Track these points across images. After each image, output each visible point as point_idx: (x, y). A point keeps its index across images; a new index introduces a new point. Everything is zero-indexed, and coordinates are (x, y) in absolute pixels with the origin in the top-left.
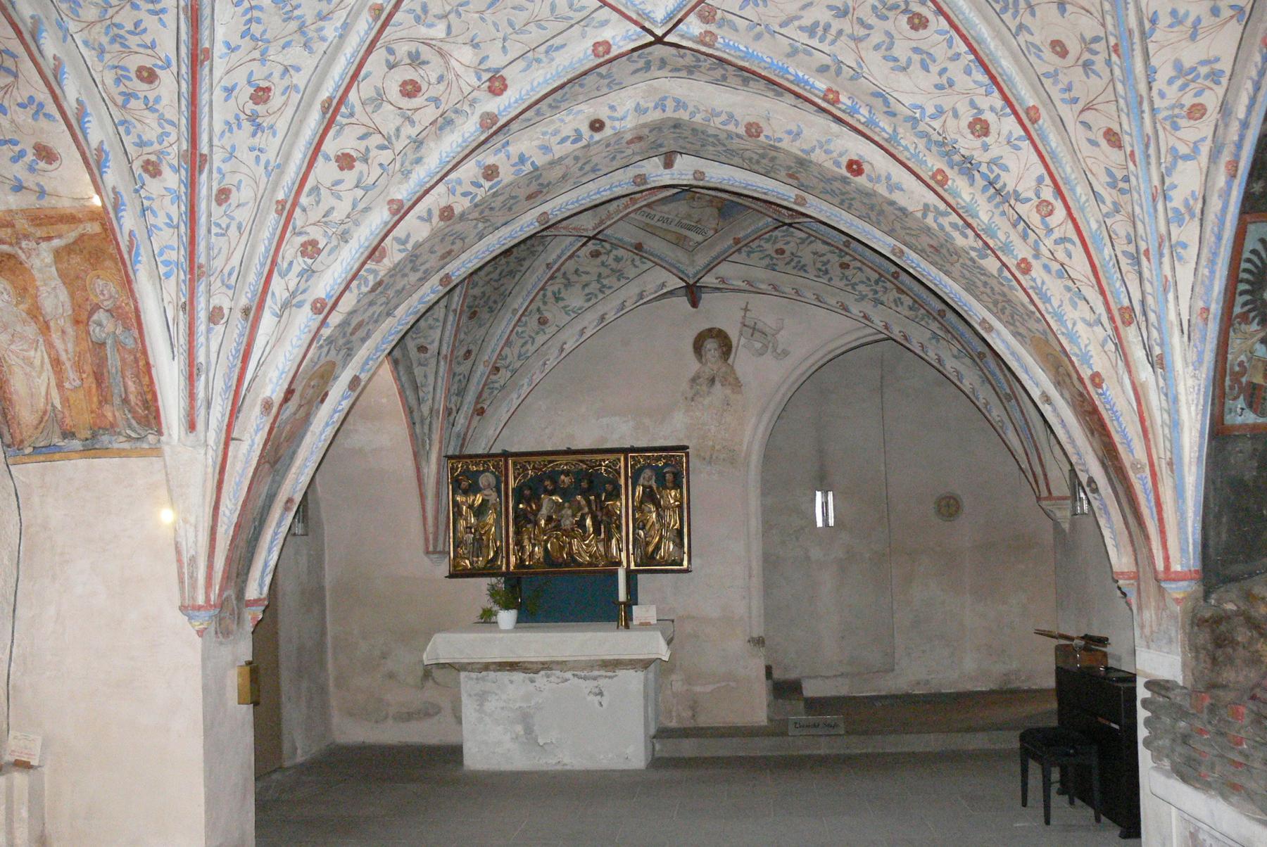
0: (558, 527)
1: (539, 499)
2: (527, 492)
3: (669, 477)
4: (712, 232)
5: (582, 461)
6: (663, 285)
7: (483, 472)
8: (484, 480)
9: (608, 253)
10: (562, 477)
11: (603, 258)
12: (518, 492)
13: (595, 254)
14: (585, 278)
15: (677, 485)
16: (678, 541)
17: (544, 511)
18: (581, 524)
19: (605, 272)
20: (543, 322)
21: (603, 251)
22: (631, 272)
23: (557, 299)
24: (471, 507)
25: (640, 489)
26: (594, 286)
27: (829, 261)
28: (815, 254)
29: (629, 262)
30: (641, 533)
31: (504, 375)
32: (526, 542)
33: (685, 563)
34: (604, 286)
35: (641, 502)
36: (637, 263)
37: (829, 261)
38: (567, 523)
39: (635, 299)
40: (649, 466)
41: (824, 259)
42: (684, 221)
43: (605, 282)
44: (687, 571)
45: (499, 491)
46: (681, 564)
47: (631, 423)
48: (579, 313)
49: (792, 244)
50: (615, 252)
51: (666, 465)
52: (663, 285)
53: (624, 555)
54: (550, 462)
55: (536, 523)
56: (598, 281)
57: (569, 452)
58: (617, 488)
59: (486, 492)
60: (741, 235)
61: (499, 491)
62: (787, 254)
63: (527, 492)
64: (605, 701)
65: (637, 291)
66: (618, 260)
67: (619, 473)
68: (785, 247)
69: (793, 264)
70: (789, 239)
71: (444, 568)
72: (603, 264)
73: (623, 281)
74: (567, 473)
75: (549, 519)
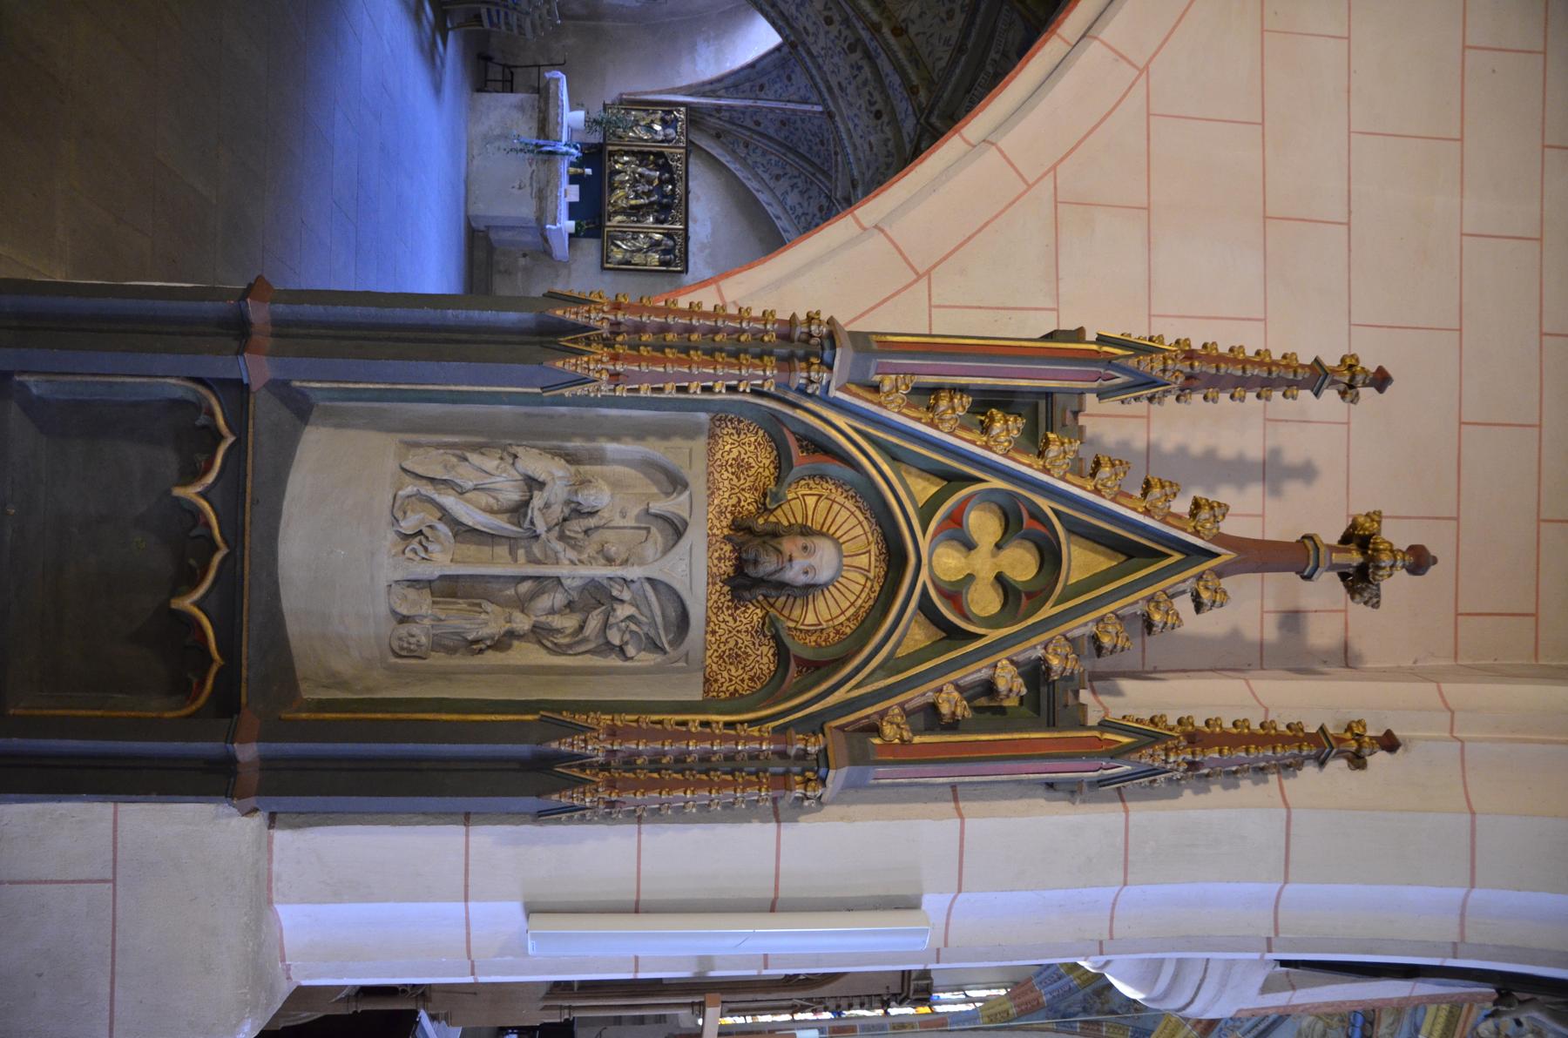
0: (636, 181)
8: (670, 131)
20: (778, 177)
23: (792, 187)
25: (657, 237)
26: (799, 211)
31: (742, 152)
38: (640, 188)
44: (603, 268)
48: (782, 203)
57: (687, 192)
64: (515, 191)
71: (608, 102)
74: (673, 190)
75: (641, 175)
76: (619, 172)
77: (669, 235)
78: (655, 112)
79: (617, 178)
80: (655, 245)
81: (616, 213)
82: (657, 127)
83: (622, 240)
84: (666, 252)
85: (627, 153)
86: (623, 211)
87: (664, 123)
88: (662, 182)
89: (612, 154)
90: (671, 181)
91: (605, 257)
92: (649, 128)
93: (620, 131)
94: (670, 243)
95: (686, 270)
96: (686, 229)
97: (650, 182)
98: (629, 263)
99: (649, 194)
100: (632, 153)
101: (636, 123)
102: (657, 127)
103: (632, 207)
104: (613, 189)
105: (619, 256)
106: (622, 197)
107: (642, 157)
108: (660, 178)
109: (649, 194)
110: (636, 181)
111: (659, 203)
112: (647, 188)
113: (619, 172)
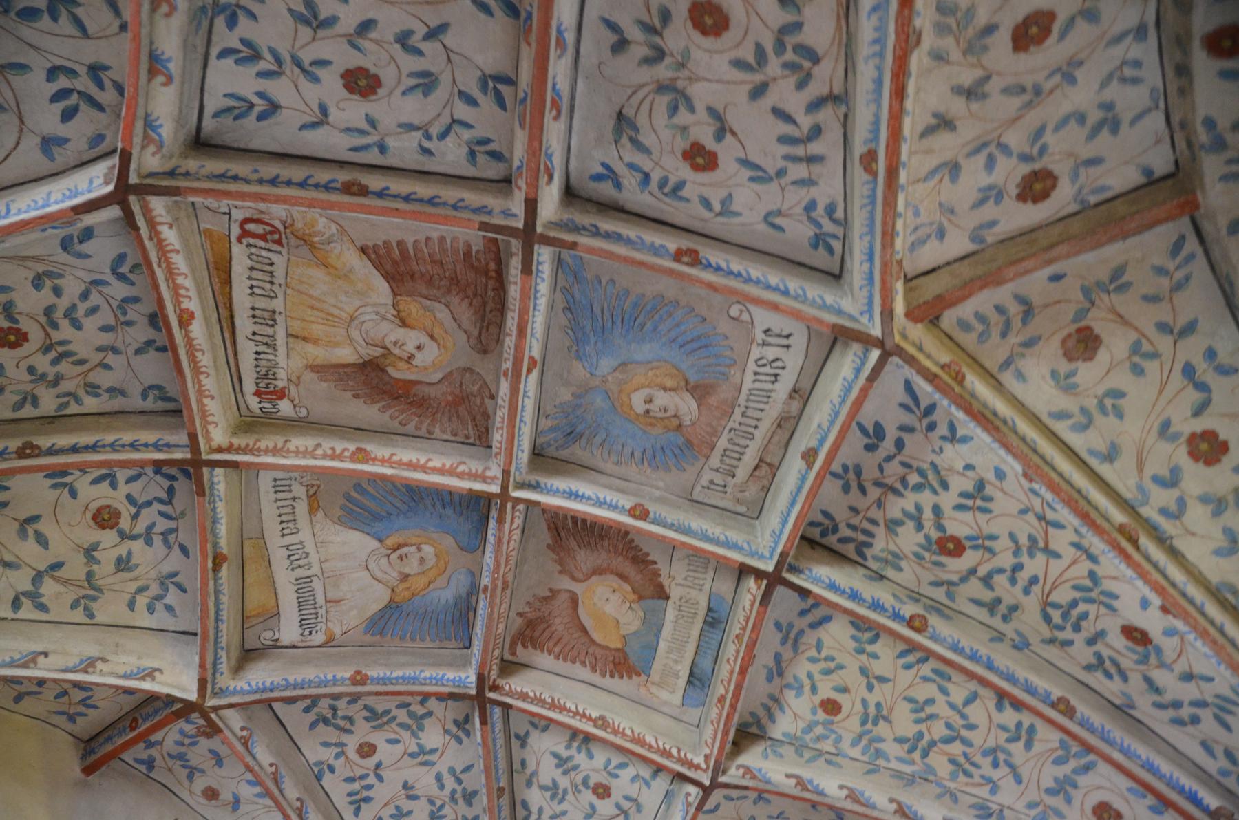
4: (319, 638)
6: (150, 674)
9: (123, 536)
11: (108, 537)
13: (104, 518)
14: (29, 550)
19: (76, 568)
21: (125, 523)
22: (110, 609)
27: (409, 813)
28: (406, 786)
29: (133, 587)
34: (34, 596)
36: (142, 601)
37: (409, 813)
39: (72, 662)
41: (406, 805)
42: (317, 585)
43: (49, 588)
49: (399, 748)
50: (137, 546)
52: (150, 674)
56: (38, 578)
60: (373, 673)
62: (371, 762)
65: (93, 651)
66: (123, 564)
68: (382, 747)
69: (356, 786)
70: (405, 735)
72: (89, 552)
73: (78, 615)
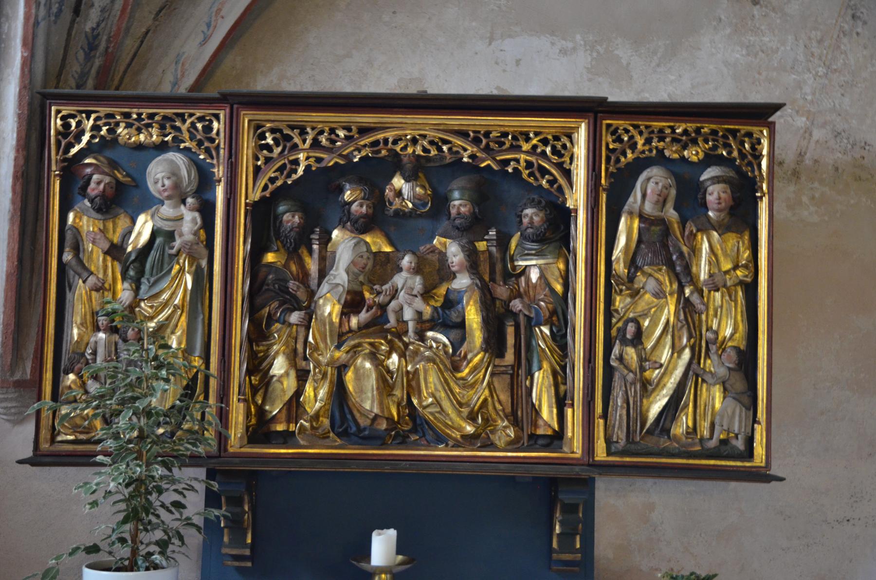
0: (377, 324)
1: (326, 238)
2: (291, 219)
3: (715, 194)
5: (463, 134)
7: (162, 147)
8: (157, 174)
10: (398, 182)
12: (263, 215)
15: (741, 216)
16: (739, 384)
17: (340, 275)
18: (447, 318)
24: (115, 251)
25: (627, 231)
30: (631, 353)
32: (279, 366)
33: (759, 450)
35: (633, 264)
40: (661, 159)
44: (762, 476)
45: (206, 210)
46: (749, 453)
47: (583, 59)
51: (710, 159)
53: (574, 417)
54: (364, 131)
55: (310, 313)
58: (560, 219)
59: (167, 210)
61: (206, 210)
63: (291, 219)
67: (568, 174)
74: (417, 170)
75: (352, 304)
76: (339, 392)
77: (614, 189)
78: (72, 241)
79: (367, 400)
80: (662, 247)
81: (521, 411)
82: (143, 228)
83: (647, 388)
84: (689, 197)
85: (258, 366)
86: (517, 381)
87: (123, 198)
88: (378, 218)
89: (260, 430)
90: (374, 172)
91: (726, 462)
92: (140, 266)
93: (164, 395)
94: (652, 184)
95: (762, 114)
96: (593, 109)
97: (380, 269)
98: (746, 360)
99: (435, 272)
100: (258, 334)
101: (120, 324)
102: (143, 228)
103: (494, 343)
104: (415, 425)
105: (717, 398)
106: (453, 391)
107: (273, 298)
108: (363, 226)
109: (435, 272)
110: (377, 324)
111: (469, 230)
112: (407, 281)
113: (339, 392)
